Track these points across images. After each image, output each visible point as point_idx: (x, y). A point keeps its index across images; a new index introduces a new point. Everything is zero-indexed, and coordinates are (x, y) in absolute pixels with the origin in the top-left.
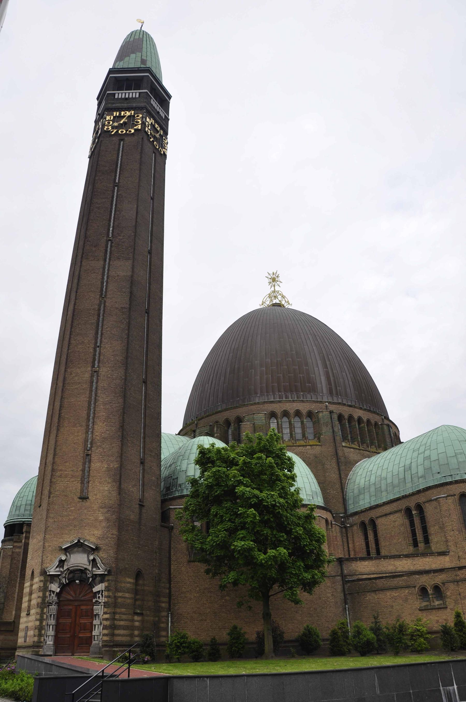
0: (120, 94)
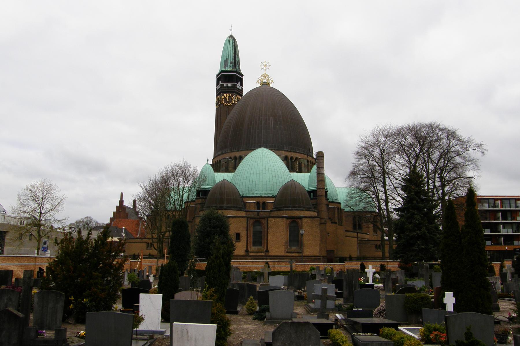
0: (226, 84)
